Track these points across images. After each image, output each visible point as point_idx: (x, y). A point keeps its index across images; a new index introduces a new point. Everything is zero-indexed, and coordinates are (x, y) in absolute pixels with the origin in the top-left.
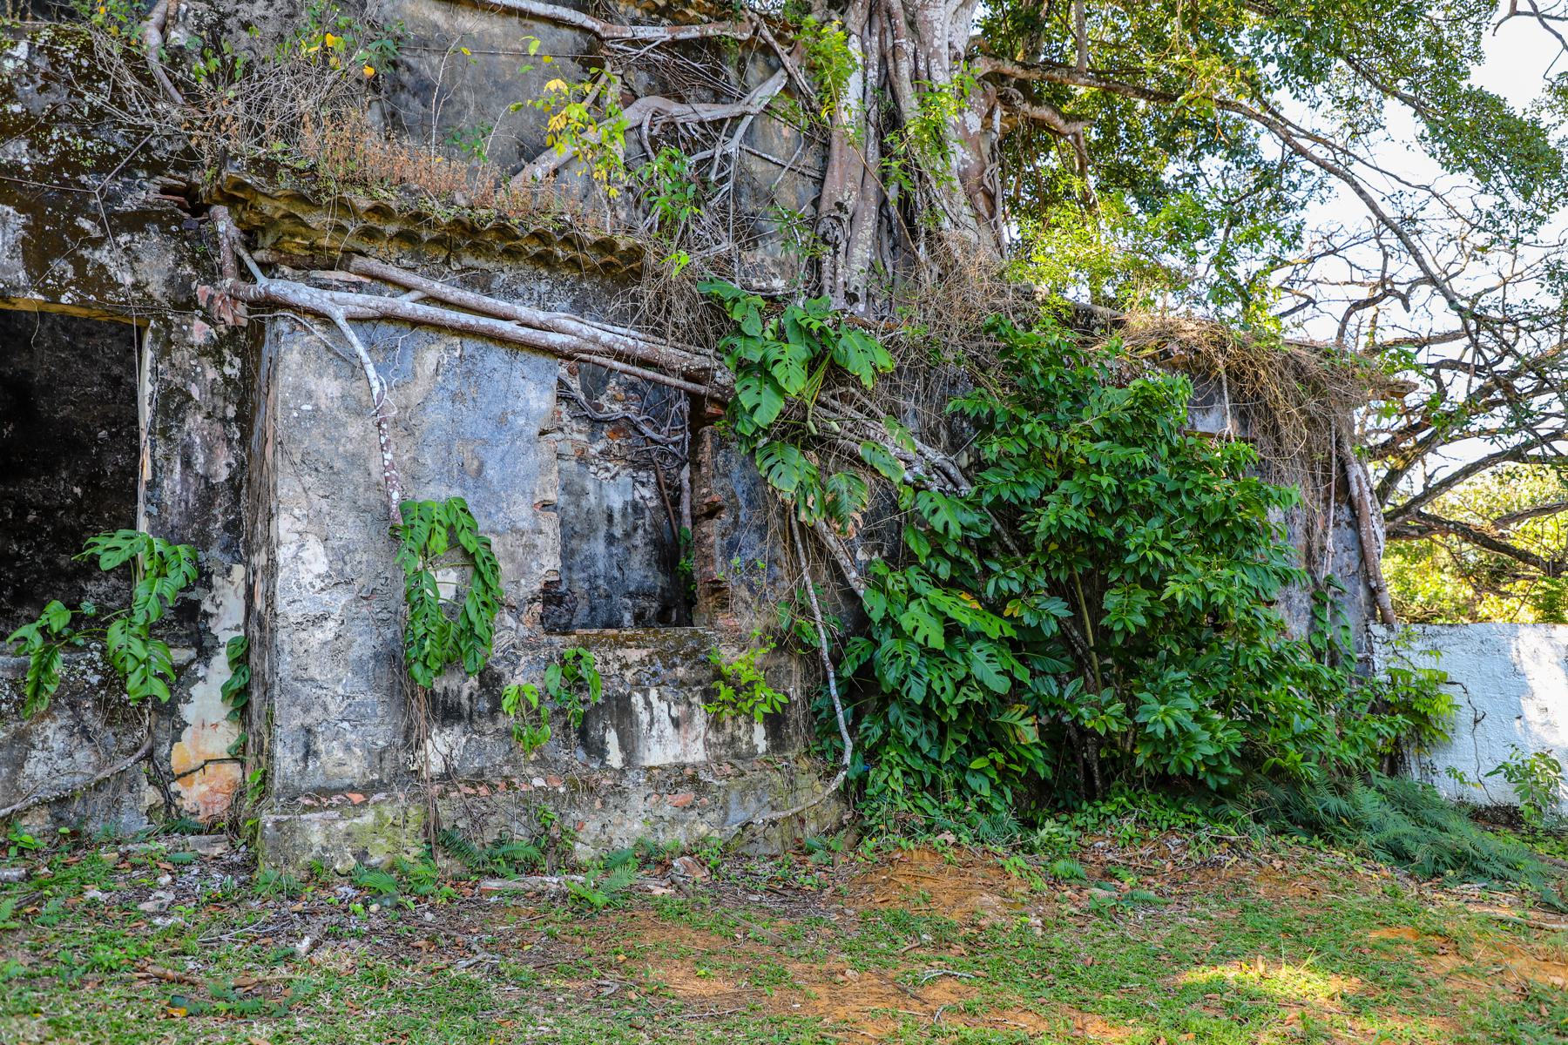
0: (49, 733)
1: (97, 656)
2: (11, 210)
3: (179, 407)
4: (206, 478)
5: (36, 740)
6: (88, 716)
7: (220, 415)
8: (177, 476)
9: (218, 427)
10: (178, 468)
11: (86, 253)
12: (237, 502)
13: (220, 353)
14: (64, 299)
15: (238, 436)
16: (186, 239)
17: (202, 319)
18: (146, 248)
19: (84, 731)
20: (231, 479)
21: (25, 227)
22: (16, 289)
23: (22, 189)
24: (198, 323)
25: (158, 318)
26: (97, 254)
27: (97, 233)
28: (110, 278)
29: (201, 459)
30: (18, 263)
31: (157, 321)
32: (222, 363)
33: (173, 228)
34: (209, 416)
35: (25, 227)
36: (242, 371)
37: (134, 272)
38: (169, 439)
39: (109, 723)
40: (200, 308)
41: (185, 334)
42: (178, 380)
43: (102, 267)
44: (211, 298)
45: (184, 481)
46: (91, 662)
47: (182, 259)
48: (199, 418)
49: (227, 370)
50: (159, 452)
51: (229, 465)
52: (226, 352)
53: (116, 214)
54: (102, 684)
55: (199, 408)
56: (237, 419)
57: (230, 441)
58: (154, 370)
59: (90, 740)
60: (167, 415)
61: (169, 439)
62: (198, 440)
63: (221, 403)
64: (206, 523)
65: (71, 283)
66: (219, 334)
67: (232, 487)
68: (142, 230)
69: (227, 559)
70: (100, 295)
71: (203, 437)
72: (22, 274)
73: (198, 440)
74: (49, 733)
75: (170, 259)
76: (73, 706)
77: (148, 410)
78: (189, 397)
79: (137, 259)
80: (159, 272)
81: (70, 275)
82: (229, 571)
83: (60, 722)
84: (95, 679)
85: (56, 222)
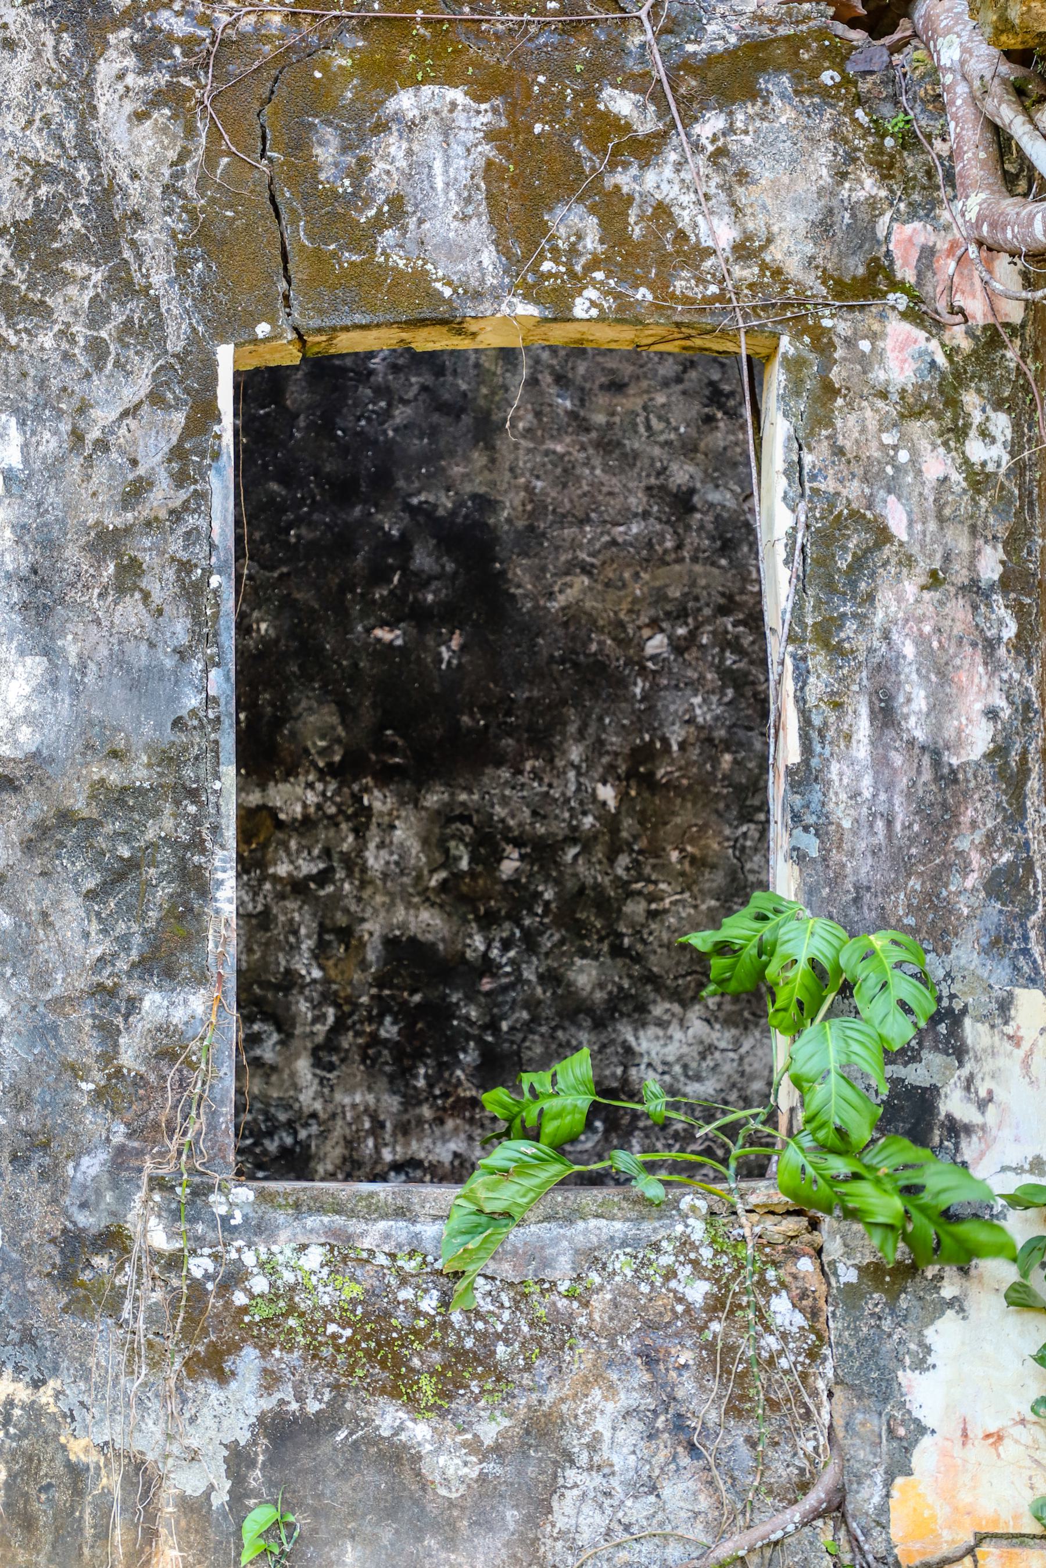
0: (602, 1425)
1: (698, 1230)
2: (457, 95)
3: (859, 563)
4: (935, 753)
5: (575, 1442)
6: (686, 1387)
7: (962, 576)
8: (862, 750)
9: (959, 610)
10: (863, 727)
11: (623, 179)
12: (1016, 815)
13: (953, 403)
14: (580, 308)
15: (1010, 631)
16: (859, 100)
17: (904, 316)
18: (764, 141)
19: (679, 1425)
20: (998, 752)
21: (491, 135)
22: (477, 296)
23: (479, 35)
24: (898, 329)
25: (800, 326)
26: (651, 177)
27: (647, 125)
28: (681, 236)
29: (920, 702)
30: (479, 229)
31: (797, 336)
32: (960, 432)
33: (829, 77)
34: (935, 580)
35: (491, 135)
36: (1015, 448)
37: (737, 210)
38: (837, 651)
39: (736, 1410)
40: (896, 285)
41: (865, 362)
42: (853, 490)
43: (663, 211)
44: (928, 254)
45: (880, 762)
46: (685, 1244)
47: (851, 158)
48: (910, 588)
49: (976, 450)
50: (816, 687)
51: (992, 714)
52: (971, 399)
53: (686, 66)
54: (716, 1305)
55: (908, 561)
56: (1005, 583)
57: (990, 645)
58: (796, 470)
59: (692, 1449)
60: (830, 587)
61: (837, 651)
62: (909, 650)
63: (963, 544)
64: (939, 876)
65: (595, 264)
66: (951, 353)
67: (1002, 773)
68: (752, 94)
69: (999, 974)
70: (661, 287)
71: (922, 640)
72: (489, 257)
73: (909, 650)
74: (602, 1425)
75: (823, 157)
76: (650, 1359)
77: (784, 574)
78: (883, 535)
79: (743, 176)
80: (798, 204)
81: (591, 243)
82: (1005, 1006)
83: (626, 1399)
84: (698, 1292)
85: (554, 111)
